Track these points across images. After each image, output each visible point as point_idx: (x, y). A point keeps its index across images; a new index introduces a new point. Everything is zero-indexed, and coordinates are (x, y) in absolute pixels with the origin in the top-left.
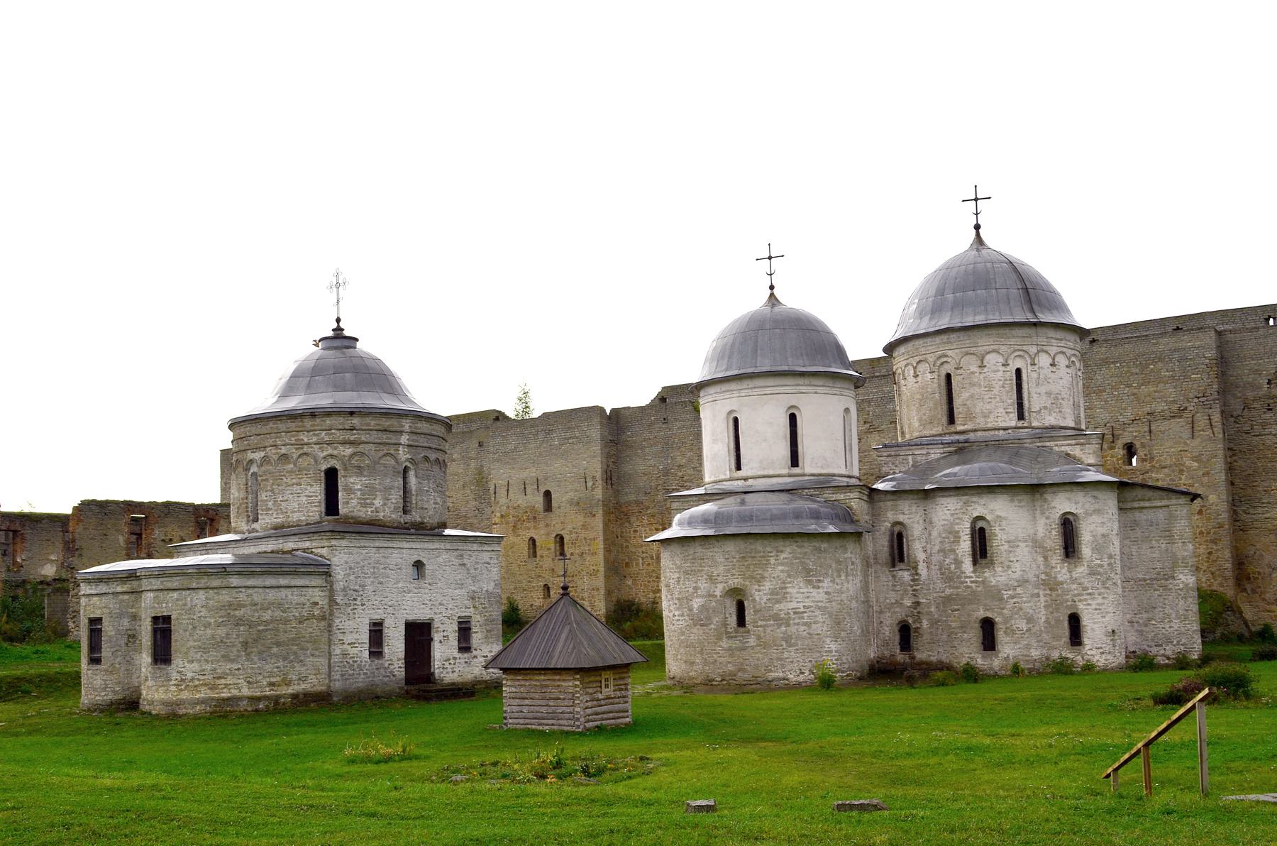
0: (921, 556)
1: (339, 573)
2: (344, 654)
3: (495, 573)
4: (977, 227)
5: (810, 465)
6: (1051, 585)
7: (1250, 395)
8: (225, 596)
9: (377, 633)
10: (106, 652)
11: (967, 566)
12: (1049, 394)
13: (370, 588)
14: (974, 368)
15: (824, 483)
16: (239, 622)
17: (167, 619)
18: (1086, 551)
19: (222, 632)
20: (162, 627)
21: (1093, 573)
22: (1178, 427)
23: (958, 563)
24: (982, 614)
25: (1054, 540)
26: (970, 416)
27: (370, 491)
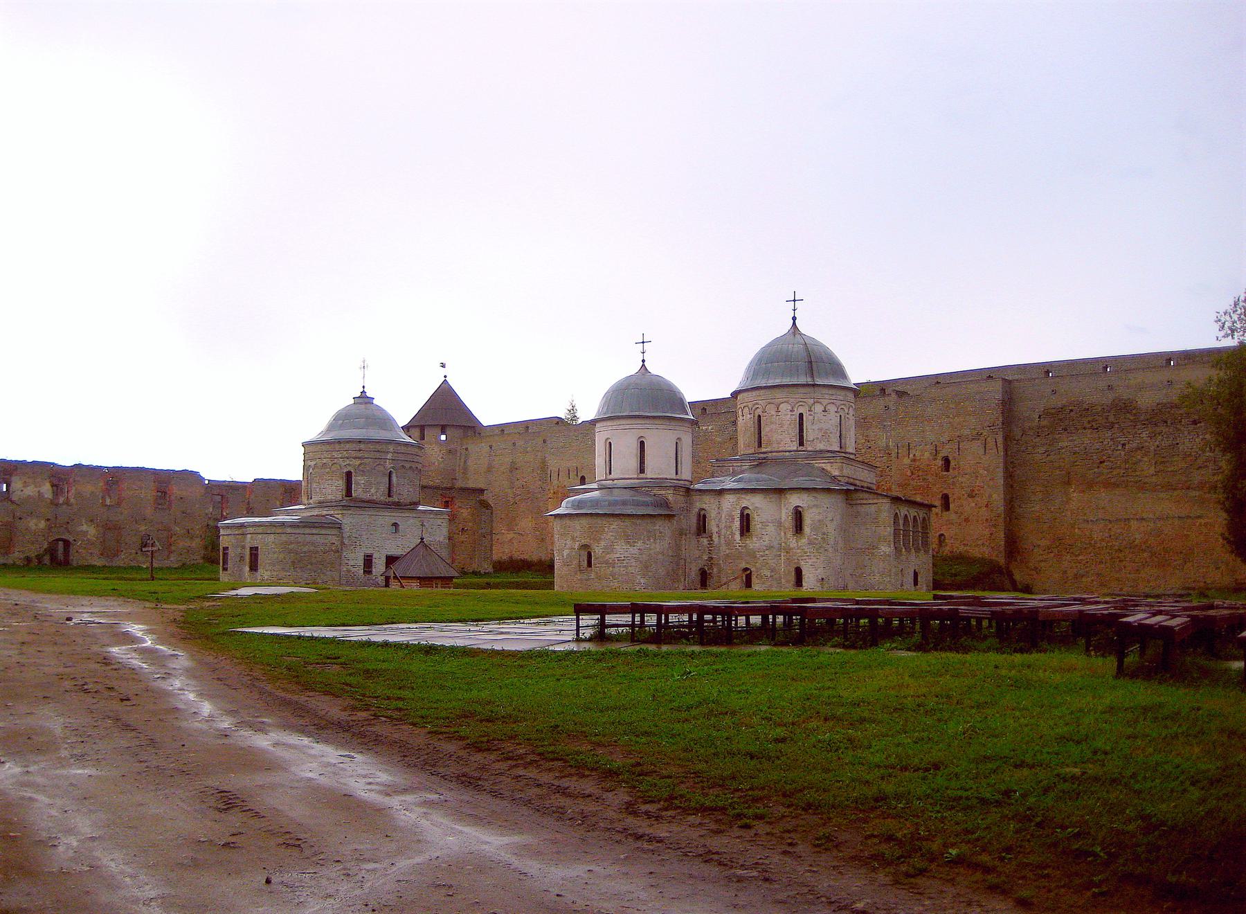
0: (715, 529)
1: (346, 528)
2: (349, 571)
4: (794, 319)
5: (650, 473)
6: (788, 550)
7: (1027, 425)
8: (284, 538)
9: (368, 561)
10: (230, 565)
11: (737, 537)
12: (821, 430)
14: (773, 413)
15: (659, 483)
19: (282, 556)
20: (254, 552)
22: (976, 447)
23: (733, 534)
24: (744, 565)
26: (769, 443)
27: (368, 485)
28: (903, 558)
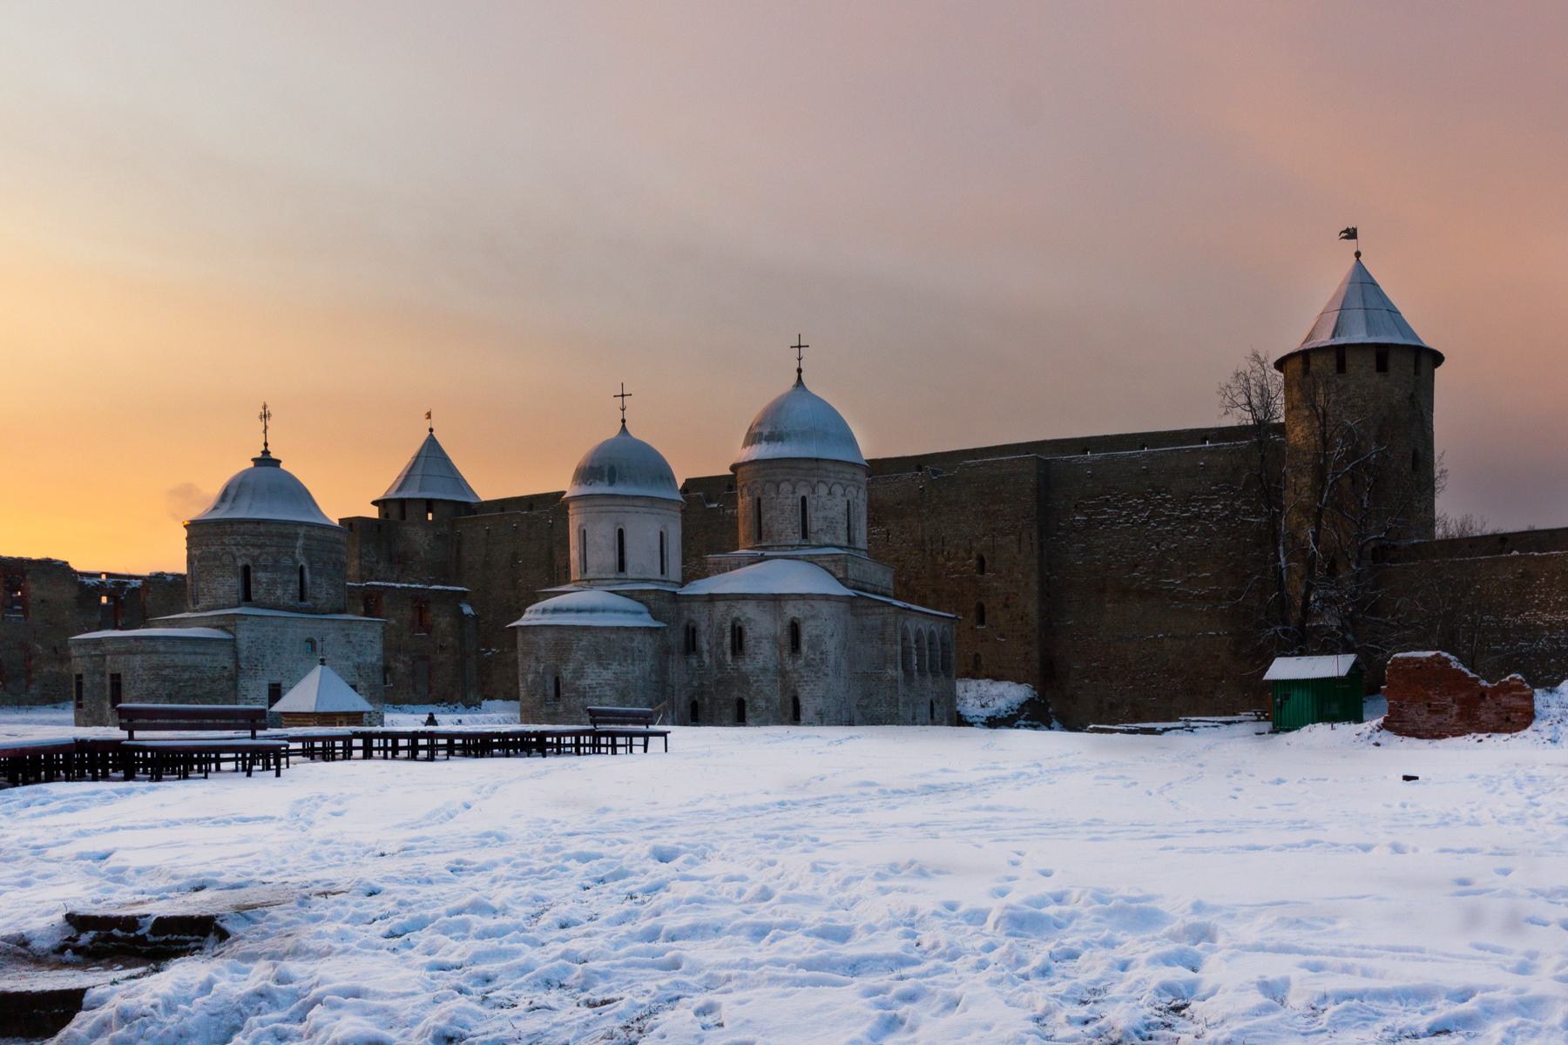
0: (705, 647)
3: (378, 647)
6: (783, 673)
11: (729, 657)
13: (269, 658)
16: (165, 679)
17: (119, 676)
18: (804, 648)
19: (153, 685)
20: (116, 680)
21: (808, 665)
23: (724, 654)
25: (785, 639)
28: (916, 684)
